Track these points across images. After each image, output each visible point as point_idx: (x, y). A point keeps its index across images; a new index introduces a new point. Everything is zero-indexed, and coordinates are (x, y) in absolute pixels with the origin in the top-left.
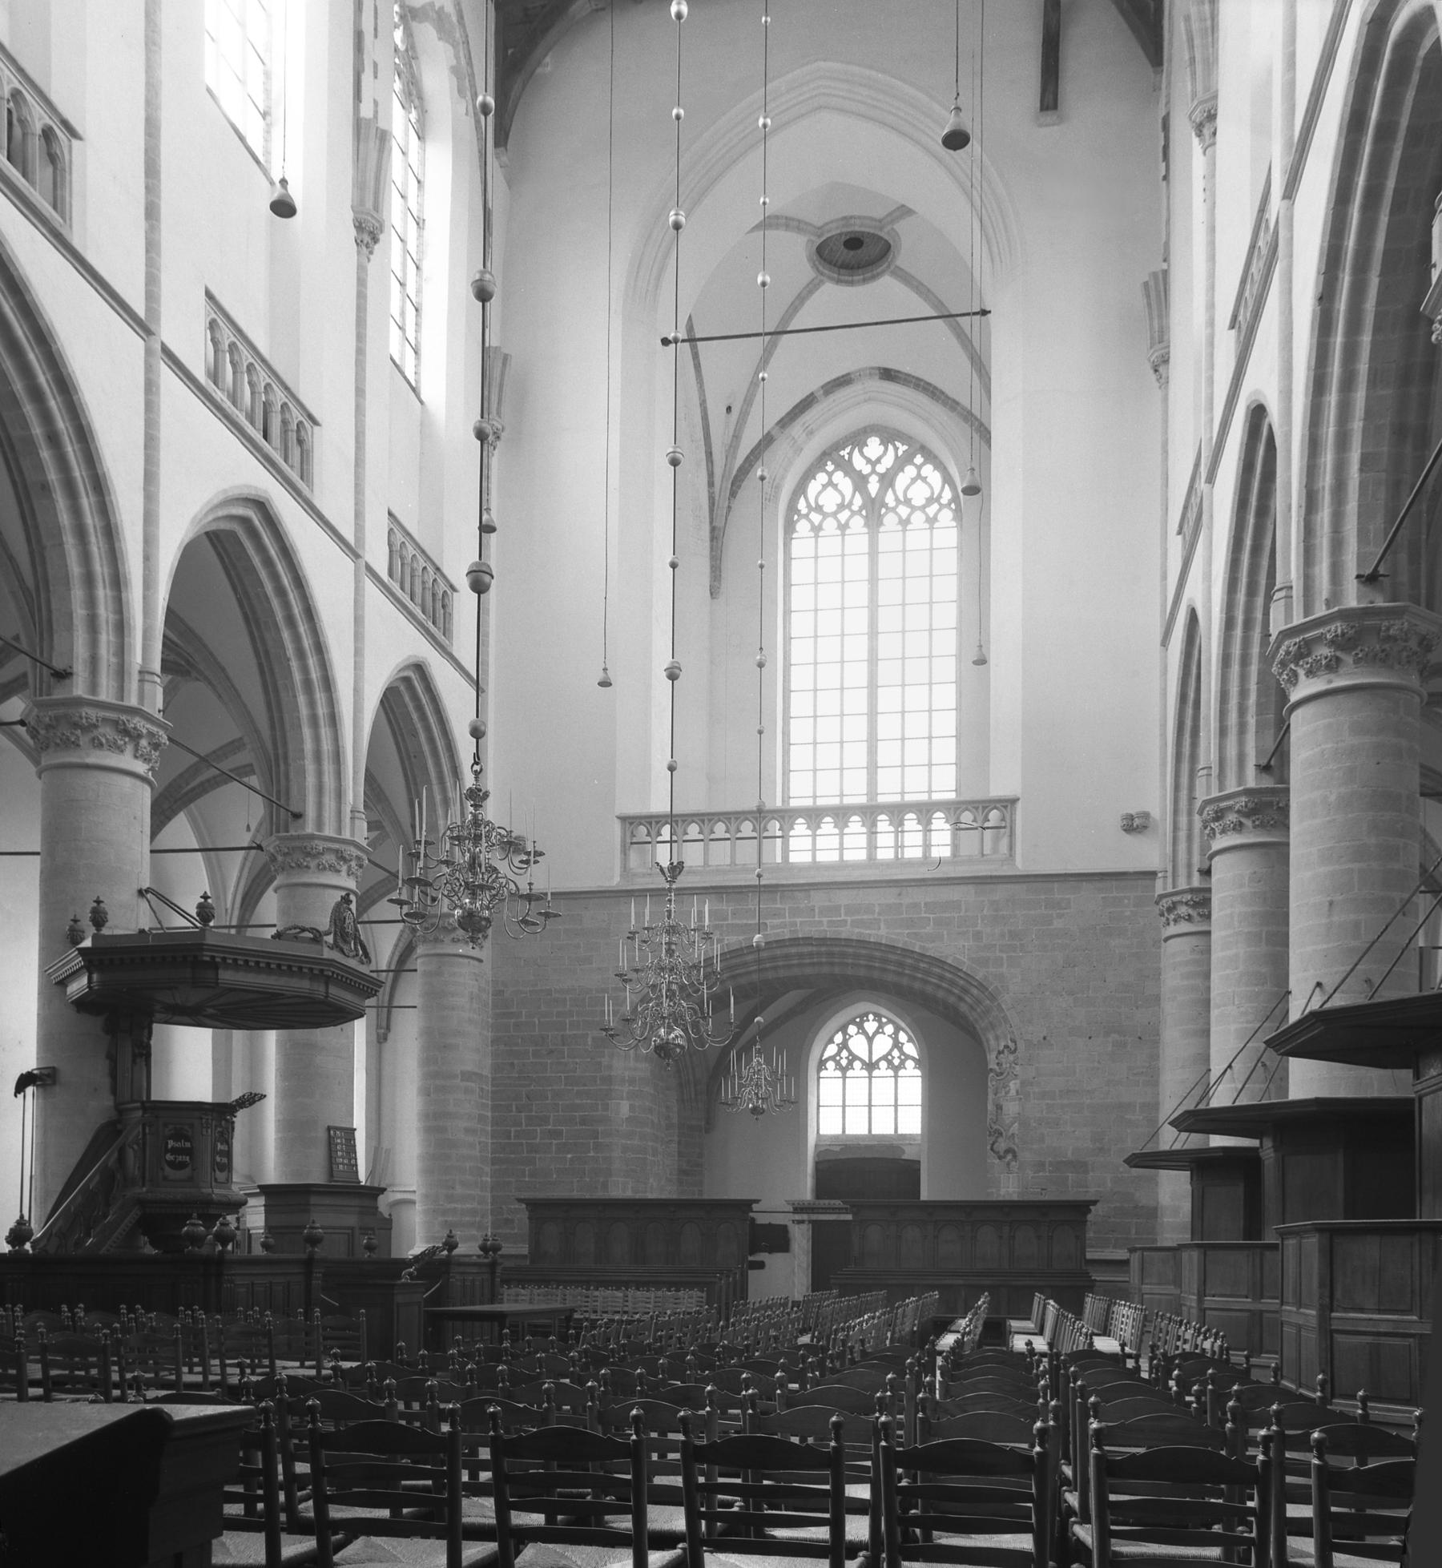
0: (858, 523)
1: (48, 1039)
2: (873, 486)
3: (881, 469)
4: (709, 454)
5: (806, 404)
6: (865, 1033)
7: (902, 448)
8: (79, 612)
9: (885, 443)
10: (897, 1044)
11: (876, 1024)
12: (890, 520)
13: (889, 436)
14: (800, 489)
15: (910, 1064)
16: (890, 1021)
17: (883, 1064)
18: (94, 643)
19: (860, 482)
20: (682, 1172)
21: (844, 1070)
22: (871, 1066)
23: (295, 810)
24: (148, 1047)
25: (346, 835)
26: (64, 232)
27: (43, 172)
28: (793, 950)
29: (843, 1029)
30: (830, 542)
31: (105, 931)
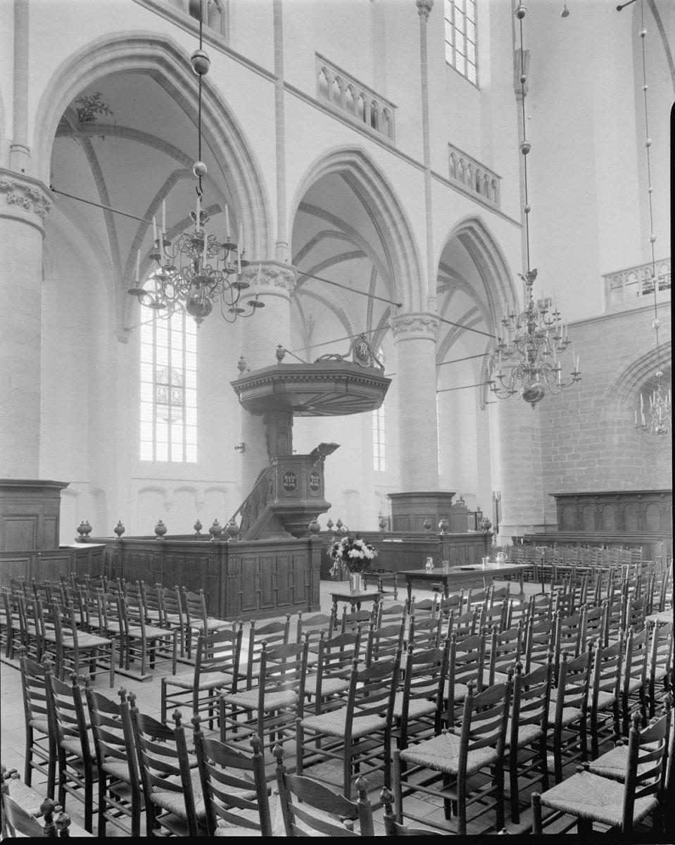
23: (398, 303)
25: (425, 310)
26: (223, 43)
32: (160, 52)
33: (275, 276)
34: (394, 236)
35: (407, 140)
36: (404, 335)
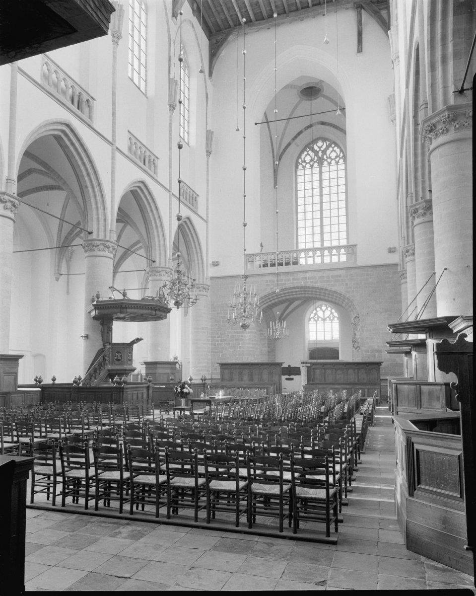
0: (316, 165)
1: (87, 328)
2: (320, 154)
3: (322, 149)
4: (273, 149)
5: (301, 132)
6: (322, 310)
7: (328, 143)
8: (95, 217)
9: (323, 142)
10: (332, 313)
11: (325, 307)
12: (325, 163)
13: (324, 140)
14: (299, 156)
15: (336, 319)
16: (329, 306)
17: (328, 319)
18: (98, 224)
19: (316, 153)
20: (269, 352)
21: (316, 321)
22: (324, 320)
23: (154, 260)
24: (111, 328)
25: (167, 266)
27: (86, 110)
28: (294, 290)
29: (316, 309)
30: (308, 171)
31: (100, 299)
32: (64, 128)
33: (108, 248)
34: (154, 225)
35: (162, 176)
36: (155, 277)
